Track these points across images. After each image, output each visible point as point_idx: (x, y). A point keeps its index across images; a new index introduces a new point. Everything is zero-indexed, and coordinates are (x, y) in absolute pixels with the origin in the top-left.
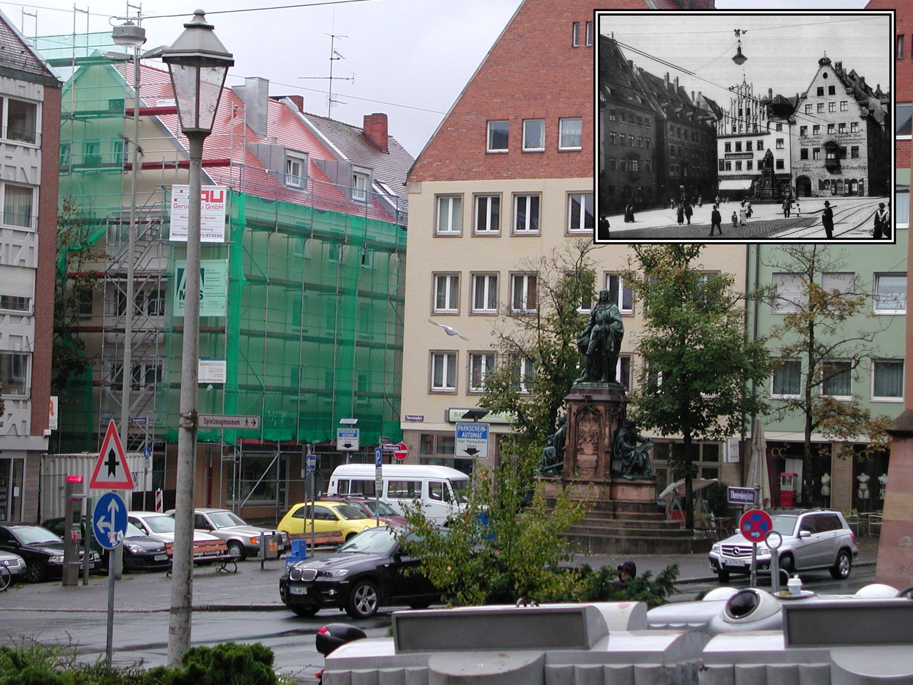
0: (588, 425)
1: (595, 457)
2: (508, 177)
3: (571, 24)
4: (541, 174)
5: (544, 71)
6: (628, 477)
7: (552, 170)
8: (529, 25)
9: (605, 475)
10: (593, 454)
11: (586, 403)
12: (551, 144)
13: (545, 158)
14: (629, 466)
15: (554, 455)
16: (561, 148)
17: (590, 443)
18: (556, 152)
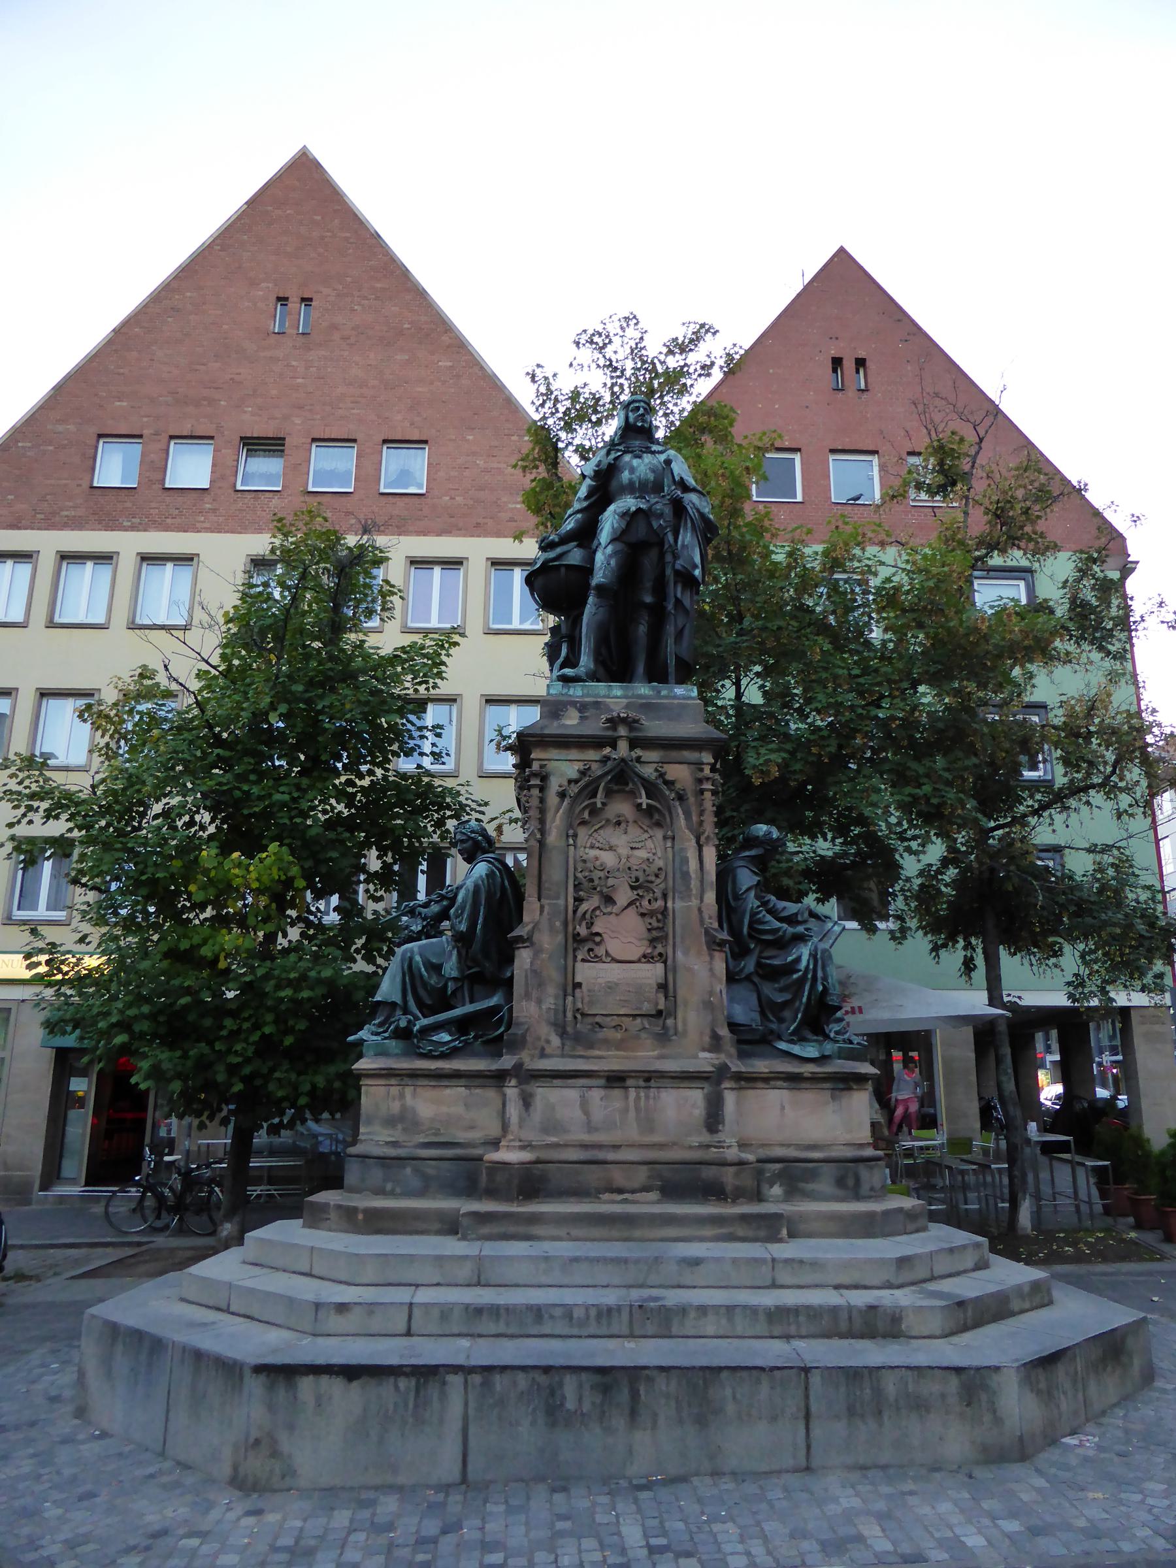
0: (620, 839)
2: (133, 528)
3: (273, 299)
4: (198, 525)
5: (218, 365)
6: (796, 1049)
7: (221, 519)
9: (715, 1044)
10: (647, 958)
11: (623, 746)
12: (223, 477)
13: (208, 498)
14: (785, 1004)
15: (451, 968)
16: (239, 487)
17: (632, 911)
18: (231, 491)
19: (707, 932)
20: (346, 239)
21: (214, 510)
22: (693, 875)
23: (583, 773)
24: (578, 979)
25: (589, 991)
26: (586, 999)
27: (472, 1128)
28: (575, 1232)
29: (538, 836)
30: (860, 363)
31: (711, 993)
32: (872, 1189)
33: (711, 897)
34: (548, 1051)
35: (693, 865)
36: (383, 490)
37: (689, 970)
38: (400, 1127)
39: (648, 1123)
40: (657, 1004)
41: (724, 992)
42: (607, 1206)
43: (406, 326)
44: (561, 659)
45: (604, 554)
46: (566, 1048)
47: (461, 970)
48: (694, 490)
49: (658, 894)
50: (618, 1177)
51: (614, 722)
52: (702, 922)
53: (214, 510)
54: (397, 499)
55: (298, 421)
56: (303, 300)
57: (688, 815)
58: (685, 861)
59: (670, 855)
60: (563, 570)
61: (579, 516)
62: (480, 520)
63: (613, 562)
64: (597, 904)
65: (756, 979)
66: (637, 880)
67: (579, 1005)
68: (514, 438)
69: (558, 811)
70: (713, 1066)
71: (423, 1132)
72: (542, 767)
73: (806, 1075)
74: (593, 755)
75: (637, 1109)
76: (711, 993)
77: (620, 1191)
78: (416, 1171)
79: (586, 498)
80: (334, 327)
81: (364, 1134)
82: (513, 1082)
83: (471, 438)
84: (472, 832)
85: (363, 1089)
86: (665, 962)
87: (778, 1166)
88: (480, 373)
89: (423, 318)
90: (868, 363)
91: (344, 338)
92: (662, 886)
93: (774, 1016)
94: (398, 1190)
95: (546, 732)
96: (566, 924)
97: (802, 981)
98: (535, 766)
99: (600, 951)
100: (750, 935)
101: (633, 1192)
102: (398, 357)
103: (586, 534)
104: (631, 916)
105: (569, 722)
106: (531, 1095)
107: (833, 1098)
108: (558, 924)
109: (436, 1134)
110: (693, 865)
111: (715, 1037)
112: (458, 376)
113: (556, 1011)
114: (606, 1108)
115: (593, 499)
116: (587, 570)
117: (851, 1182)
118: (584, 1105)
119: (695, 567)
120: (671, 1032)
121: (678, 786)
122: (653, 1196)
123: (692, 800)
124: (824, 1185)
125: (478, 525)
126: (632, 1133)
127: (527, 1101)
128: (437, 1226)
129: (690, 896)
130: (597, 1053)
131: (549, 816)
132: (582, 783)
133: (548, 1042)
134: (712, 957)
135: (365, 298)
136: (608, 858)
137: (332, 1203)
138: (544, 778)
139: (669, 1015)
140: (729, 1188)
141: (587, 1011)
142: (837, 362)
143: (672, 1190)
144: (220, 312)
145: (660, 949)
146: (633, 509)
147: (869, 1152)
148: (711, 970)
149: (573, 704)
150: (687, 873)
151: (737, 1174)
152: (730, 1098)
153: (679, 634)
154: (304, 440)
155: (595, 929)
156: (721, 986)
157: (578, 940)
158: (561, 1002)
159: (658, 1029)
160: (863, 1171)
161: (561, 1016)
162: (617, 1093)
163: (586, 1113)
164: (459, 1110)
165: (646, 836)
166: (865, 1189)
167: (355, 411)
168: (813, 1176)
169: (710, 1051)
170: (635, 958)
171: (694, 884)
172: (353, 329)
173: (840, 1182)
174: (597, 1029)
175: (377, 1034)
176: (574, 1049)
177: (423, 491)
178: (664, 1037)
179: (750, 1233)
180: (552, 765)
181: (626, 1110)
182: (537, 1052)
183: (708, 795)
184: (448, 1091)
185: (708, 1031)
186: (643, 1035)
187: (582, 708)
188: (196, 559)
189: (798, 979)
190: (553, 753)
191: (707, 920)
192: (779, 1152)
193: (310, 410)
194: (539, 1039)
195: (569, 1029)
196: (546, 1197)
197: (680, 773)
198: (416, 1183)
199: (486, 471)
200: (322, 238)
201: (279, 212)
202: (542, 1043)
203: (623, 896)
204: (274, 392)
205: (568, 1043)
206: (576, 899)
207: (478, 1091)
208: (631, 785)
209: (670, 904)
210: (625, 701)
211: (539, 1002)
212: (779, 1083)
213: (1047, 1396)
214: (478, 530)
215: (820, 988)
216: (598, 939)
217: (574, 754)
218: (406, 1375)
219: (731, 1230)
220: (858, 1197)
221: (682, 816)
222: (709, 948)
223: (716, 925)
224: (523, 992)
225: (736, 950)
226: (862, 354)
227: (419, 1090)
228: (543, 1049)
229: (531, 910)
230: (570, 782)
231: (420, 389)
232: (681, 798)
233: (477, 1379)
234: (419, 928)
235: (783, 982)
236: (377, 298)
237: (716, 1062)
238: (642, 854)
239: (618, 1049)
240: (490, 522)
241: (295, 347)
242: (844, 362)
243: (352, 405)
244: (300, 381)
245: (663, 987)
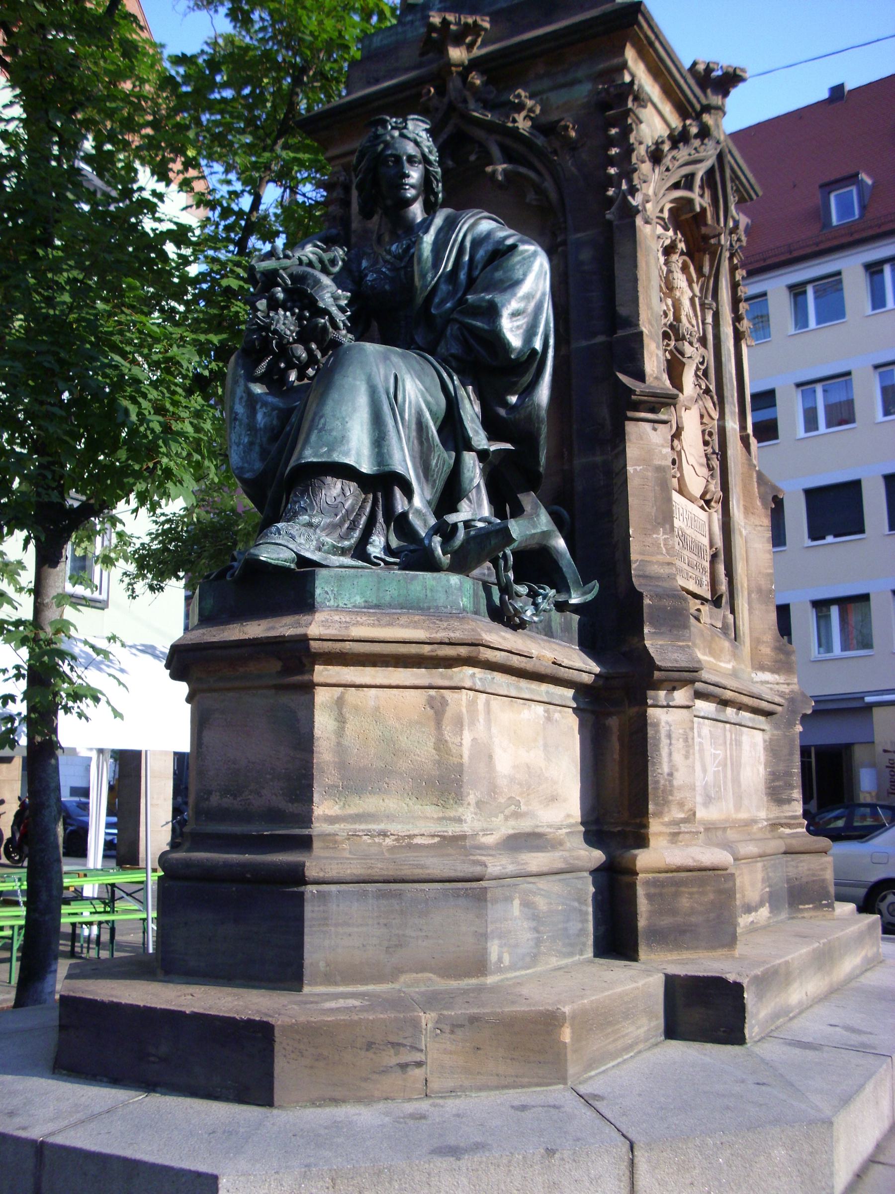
70: (781, 694)
81: (332, 820)
85: (322, 696)
109: (516, 815)
137: (567, 1009)
169: (773, 671)
224: (651, 509)
227: (495, 702)
237: (785, 689)
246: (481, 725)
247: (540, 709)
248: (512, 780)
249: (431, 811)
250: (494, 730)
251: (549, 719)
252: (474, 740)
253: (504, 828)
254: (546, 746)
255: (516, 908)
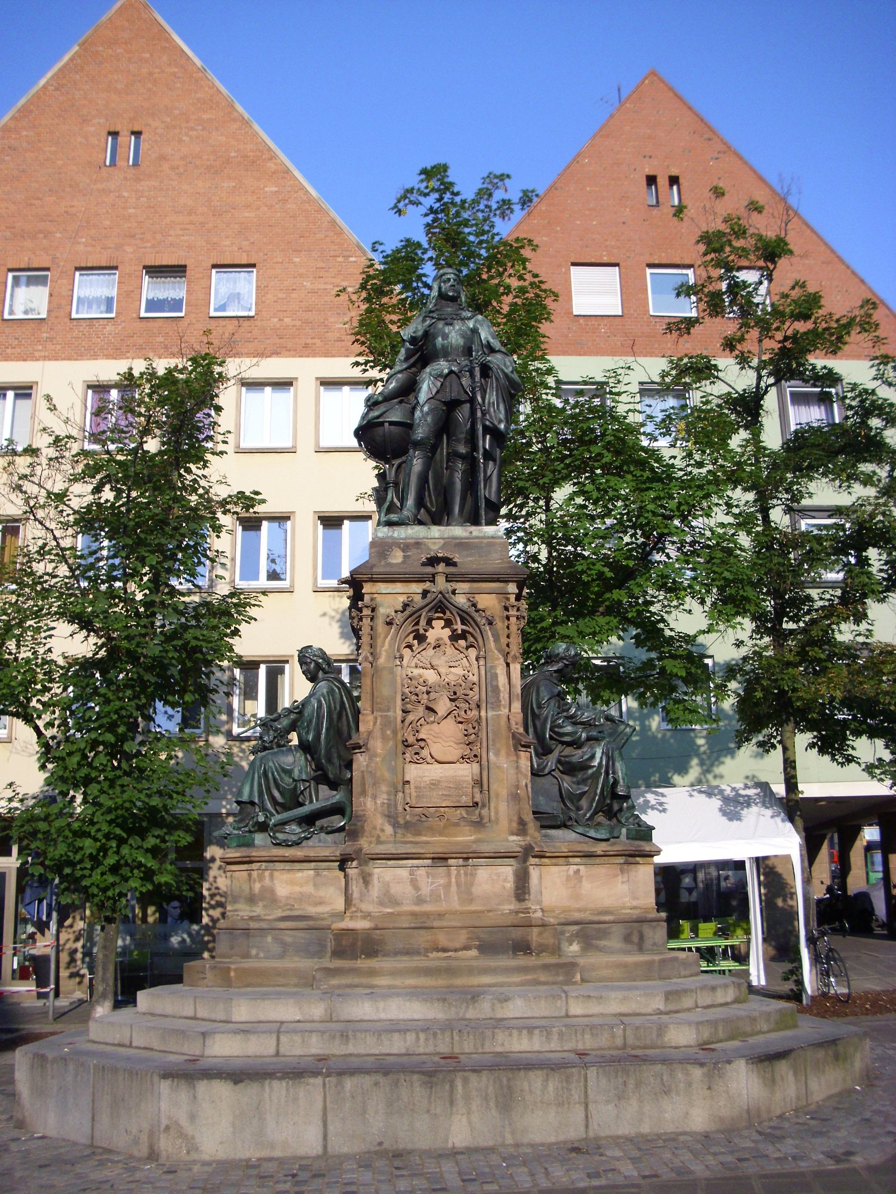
1: (466, 771)
3: (105, 133)
4: (37, 354)
5: (54, 198)
7: (59, 347)
8: (31, 133)
12: (59, 307)
13: (45, 328)
16: (74, 316)
17: (450, 721)
18: (67, 320)
19: (514, 736)
20: (174, 74)
21: (51, 339)
22: (502, 689)
23: (406, 606)
24: (407, 779)
25: (416, 788)
26: (414, 794)
27: (321, 903)
28: (411, 981)
29: (371, 659)
30: (674, 180)
31: (517, 787)
32: (655, 944)
33: (517, 706)
34: (383, 838)
35: (502, 680)
36: (213, 313)
37: (499, 767)
38: (260, 904)
39: (467, 895)
40: (473, 797)
41: (529, 786)
42: (435, 959)
43: (233, 154)
44: (387, 504)
45: (422, 411)
46: (399, 835)
47: (307, 773)
48: (499, 351)
49: (473, 706)
50: (443, 939)
51: (433, 561)
52: (509, 728)
53: (51, 339)
54: (227, 321)
55: (129, 249)
56: (133, 133)
57: (497, 638)
58: (495, 676)
59: (483, 672)
60: (386, 425)
61: (399, 376)
62: (309, 341)
63: (429, 419)
64: (421, 715)
65: (557, 774)
66: (455, 693)
67: (408, 800)
68: (340, 259)
69: (386, 637)
70: (521, 846)
71: (280, 907)
72: (372, 599)
73: (599, 853)
74: (417, 588)
75: (458, 885)
76: (517, 787)
77: (445, 950)
78: (275, 939)
79: (406, 359)
80: (163, 158)
82: (355, 863)
83: (298, 260)
84: (315, 656)
86: (479, 762)
87: (576, 928)
88: (305, 198)
89: (249, 147)
90: (681, 181)
91: (173, 168)
92: (476, 698)
93: (572, 802)
94: (262, 955)
95: (375, 570)
96: (395, 732)
97: (597, 774)
98: (367, 598)
99: (425, 753)
100: (551, 738)
101: (456, 950)
102: (226, 185)
103: (408, 389)
104: (450, 723)
105: (394, 561)
106: (370, 875)
107: (622, 871)
108: (388, 732)
110: (502, 680)
111: (522, 823)
112: (284, 201)
113: (389, 805)
114: (432, 883)
115: (412, 360)
116: (408, 426)
117: (635, 939)
118: (414, 883)
119: (500, 421)
120: (486, 820)
121: (488, 613)
122: (474, 953)
123: (500, 625)
124: (614, 942)
125: (306, 346)
126: (455, 903)
127: (366, 879)
128: (295, 980)
129: (499, 706)
130: (424, 838)
131: (379, 641)
132: (407, 613)
133: (383, 830)
134: (518, 757)
135: (192, 129)
136: (431, 676)
138: (373, 610)
139: (484, 806)
140: (534, 945)
141: (413, 803)
142: (651, 180)
143: (487, 948)
144: (54, 149)
145: (476, 749)
146: (446, 371)
147: (654, 914)
148: (517, 767)
149: (398, 545)
150: (497, 687)
151: (540, 934)
152: (534, 873)
153: (488, 479)
154: (136, 268)
155: (421, 736)
156: (526, 779)
157: (406, 745)
158: (392, 797)
159: (475, 818)
160: (647, 930)
161: (392, 810)
162: (442, 870)
163: (417, 888)
164: (309, 889)
165: (462, 655)
166: (648, 944)
167: (185, 238)
168: (604, 934)
169: (517, 835)
170: (455, 760)
171: (504, 695)
172: (183, 158)
173: (627, 939)
174: (424, 819)
175: (239, 829)
176: (404, 835)
177: (252, 313)
178: (479, 824)
179: (551, 979)
180: (379, 598)
181: (448, 885)
182: (374, 839)
183: (513, 620)
184: (300, 874)
185: (516, 818)
186: (462, 823)
187: (406, 547)
188: (34, 387)
189: (593, 773)
190: (383, 587)
191: (514, 726)
192: (577, 916)
193: (142, 239)
194: (375, 828)
195: (401, 821)
196: (384, 956)
197: (488, 601)
198: (276, 949)
199: (313, 292)
200: (151, 74)
201: (110, 52)
202: (378, 832)
203: (443, 706)
204: (107, 223)
205: (400, 831)
206: (404, 711)
207: (325, 873)
208: (448, 613)
209: (483, 713)
210: (442, 541)
211: (374, 797)
212: (578, 860)
213: (771, 1082)
214: (307, 350)
215: (611, 780)
216: (422, 744)
217: (399, 587)
218: (280, 1079)
219: (535, 976)
220: (641, 949)
221: (491, 639)
222: (516, 749)
223: (521, 730)
224: (359, 789)
225: (540, 751)
226: (674, 172)
227: (276, 874)
228: (379, 837)
229: (367, 723)
230: (396, 612)
231: (247, 215)
232: (490, 623)
233: (333, 1080)
234: (271, 738)
235: (580, 776)
236: (204, 129)
237: (523, 843)
238: (459, 671)
239: (441, 834)
240: (317, 341)
241: (125, 179)
242: (658, 180)
243: (181, 232)
244: (132, 211)
245: (479, 783)
246: (267, 881)
247: (312, 872)
248: (288, 898)
249: (248, 908)
250: (276, 882)
251: (318, 875)
252: (263, 886)
253: (279, 913)
254: (315, 885)
255: (269, 939)
